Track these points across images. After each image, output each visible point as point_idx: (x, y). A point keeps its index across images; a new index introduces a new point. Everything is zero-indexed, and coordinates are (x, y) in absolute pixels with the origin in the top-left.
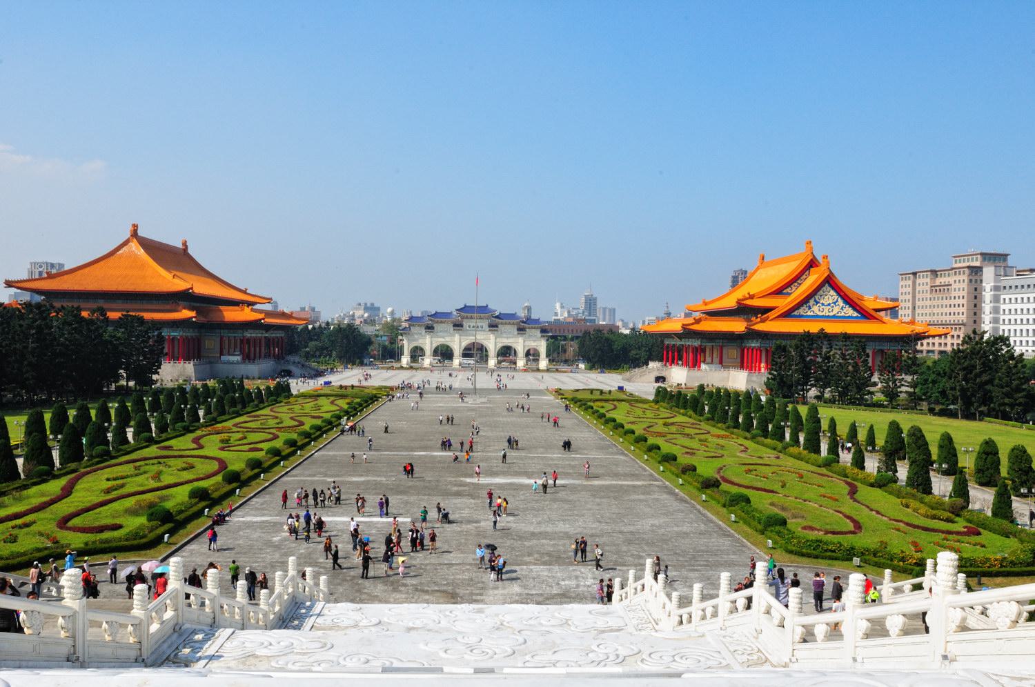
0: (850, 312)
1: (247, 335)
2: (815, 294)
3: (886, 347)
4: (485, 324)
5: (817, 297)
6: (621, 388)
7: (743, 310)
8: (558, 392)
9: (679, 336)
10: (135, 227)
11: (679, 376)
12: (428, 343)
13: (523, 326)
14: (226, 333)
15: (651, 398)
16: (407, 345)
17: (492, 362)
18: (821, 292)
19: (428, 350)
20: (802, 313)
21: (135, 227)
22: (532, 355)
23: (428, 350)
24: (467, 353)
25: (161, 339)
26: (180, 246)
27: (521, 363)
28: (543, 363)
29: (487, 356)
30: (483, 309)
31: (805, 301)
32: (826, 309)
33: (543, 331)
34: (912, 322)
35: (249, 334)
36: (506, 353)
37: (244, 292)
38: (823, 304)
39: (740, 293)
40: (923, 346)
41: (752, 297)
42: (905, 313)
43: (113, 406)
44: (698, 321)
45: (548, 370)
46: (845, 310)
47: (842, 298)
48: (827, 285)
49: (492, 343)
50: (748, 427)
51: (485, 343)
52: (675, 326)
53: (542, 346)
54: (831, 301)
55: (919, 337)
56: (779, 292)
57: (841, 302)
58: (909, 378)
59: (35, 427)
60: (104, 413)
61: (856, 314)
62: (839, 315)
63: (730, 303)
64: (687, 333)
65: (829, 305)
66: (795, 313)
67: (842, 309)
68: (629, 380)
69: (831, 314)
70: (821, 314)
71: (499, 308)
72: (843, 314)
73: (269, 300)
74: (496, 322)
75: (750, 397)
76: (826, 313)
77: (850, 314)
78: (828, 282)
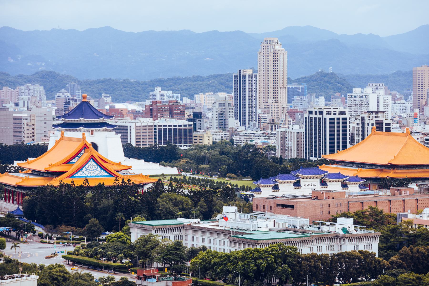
0: (104, 173)
2: (86, 165)
5: (86, 167)
18: (88, 164)
20: (79, 175)
31: (80, 169)
32: (92, 172)
38: (90, 170)
46: (101, 173)
47: (100, 167)
48: (92, 160)
54: (94, 168)
57: (99, 168)
61: (107, 174)
62: (99, 175)
65: (93, 170)
66: (76, 175)
67: (100, 172)
69: (94, 175)
70: (89, 175)
72: (100, 175)
76: (92, 174)
77: (104, 175)
78: (92, 158)
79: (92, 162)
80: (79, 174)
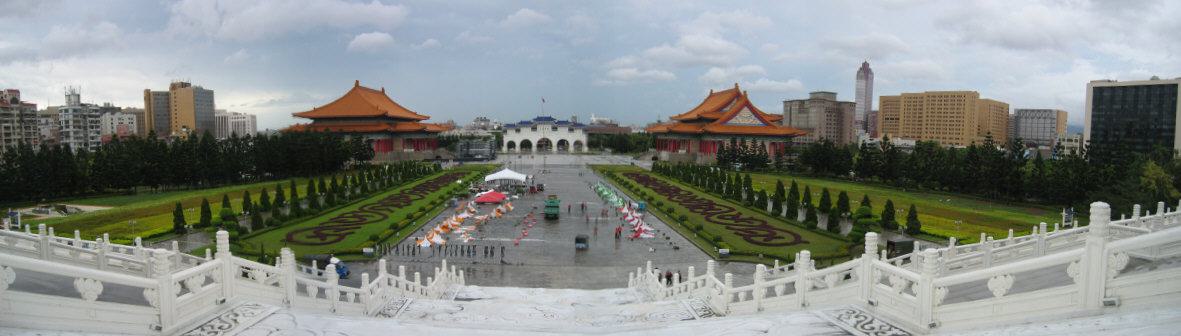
1: (418, 137)
3: (775, 140)
4: (550, 127)
6: (632, 164)
7: (700, 120)
8: (593, 167)
9: (665, 134)
10: (357, 82)
11: (664, 155)
12: (518, 139)
13: (573, 126)
14: (406, 137)
15: (650, 169)
16: (506, 139)
17: (555, 149)
19: (518, 144)
21: (357, 82)
22: (578, 144)
23: (518, 144)
24: (540, 145)
25: (370, 142)
26: (380, 89)
27: (571, 148)
28: (585, 149)
29: (551, 146)
30: (549, 119)
33: (585, 131)
34: (790, 127)
35: (418, 137)
36: (562, 143)
37: (415, 114)
39: (700, 111)
40: (795, 140)
41: (705, 113)
42: (786, 123)
43: (349, 178)
44: (675, 125)
45: (588, 154)
49: (554, 138)
50: (703, 185)
51: (551, 138)
52: (664, 129)
53: (582, 137)
55: (792, 136)
56: (720, 109)
57: (753, 117)
58: (788, 158)
59: (311, 189)
60: (345, 182)
63: (694, 116)
64: (670, 132)
68: (636, 158)
71: (559, 118)
73: (428, 118)
74: (557, 125)
75: (702, 171)
79: (746, 108)
80: (733, 121)
